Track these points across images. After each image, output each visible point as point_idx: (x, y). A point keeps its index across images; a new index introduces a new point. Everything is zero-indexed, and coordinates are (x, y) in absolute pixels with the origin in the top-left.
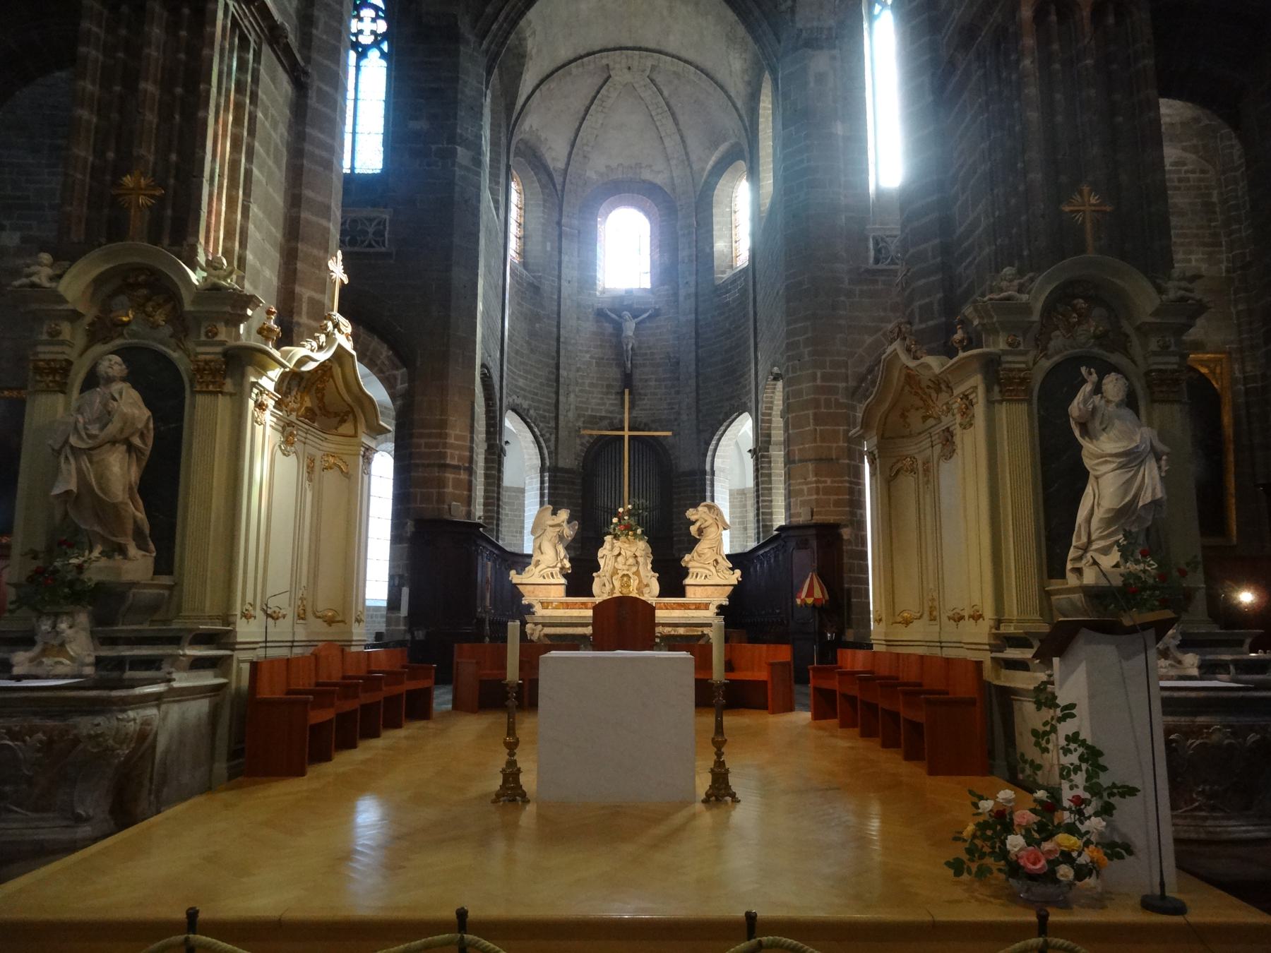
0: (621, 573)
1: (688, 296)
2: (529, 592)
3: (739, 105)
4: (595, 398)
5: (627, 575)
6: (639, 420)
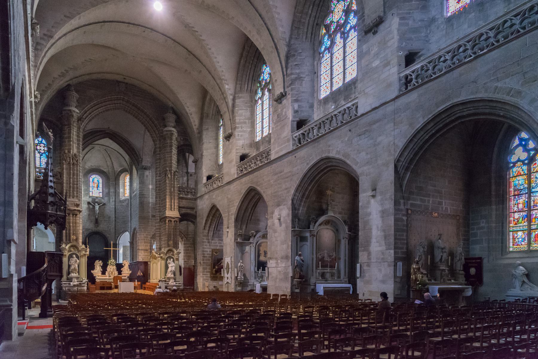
3: (128, 163)
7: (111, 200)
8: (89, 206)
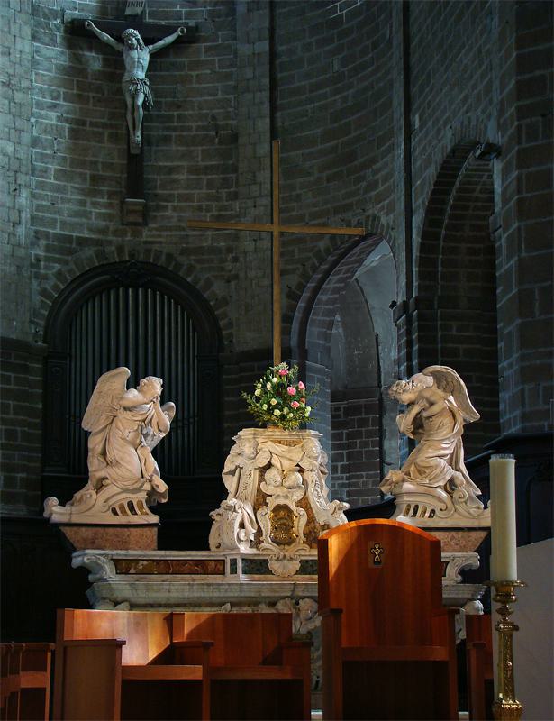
0: (272, 502)
2: (85, 540)
4: (69, 201)
5: (286, 507)
6: (156, 247)
8: (76, 58)
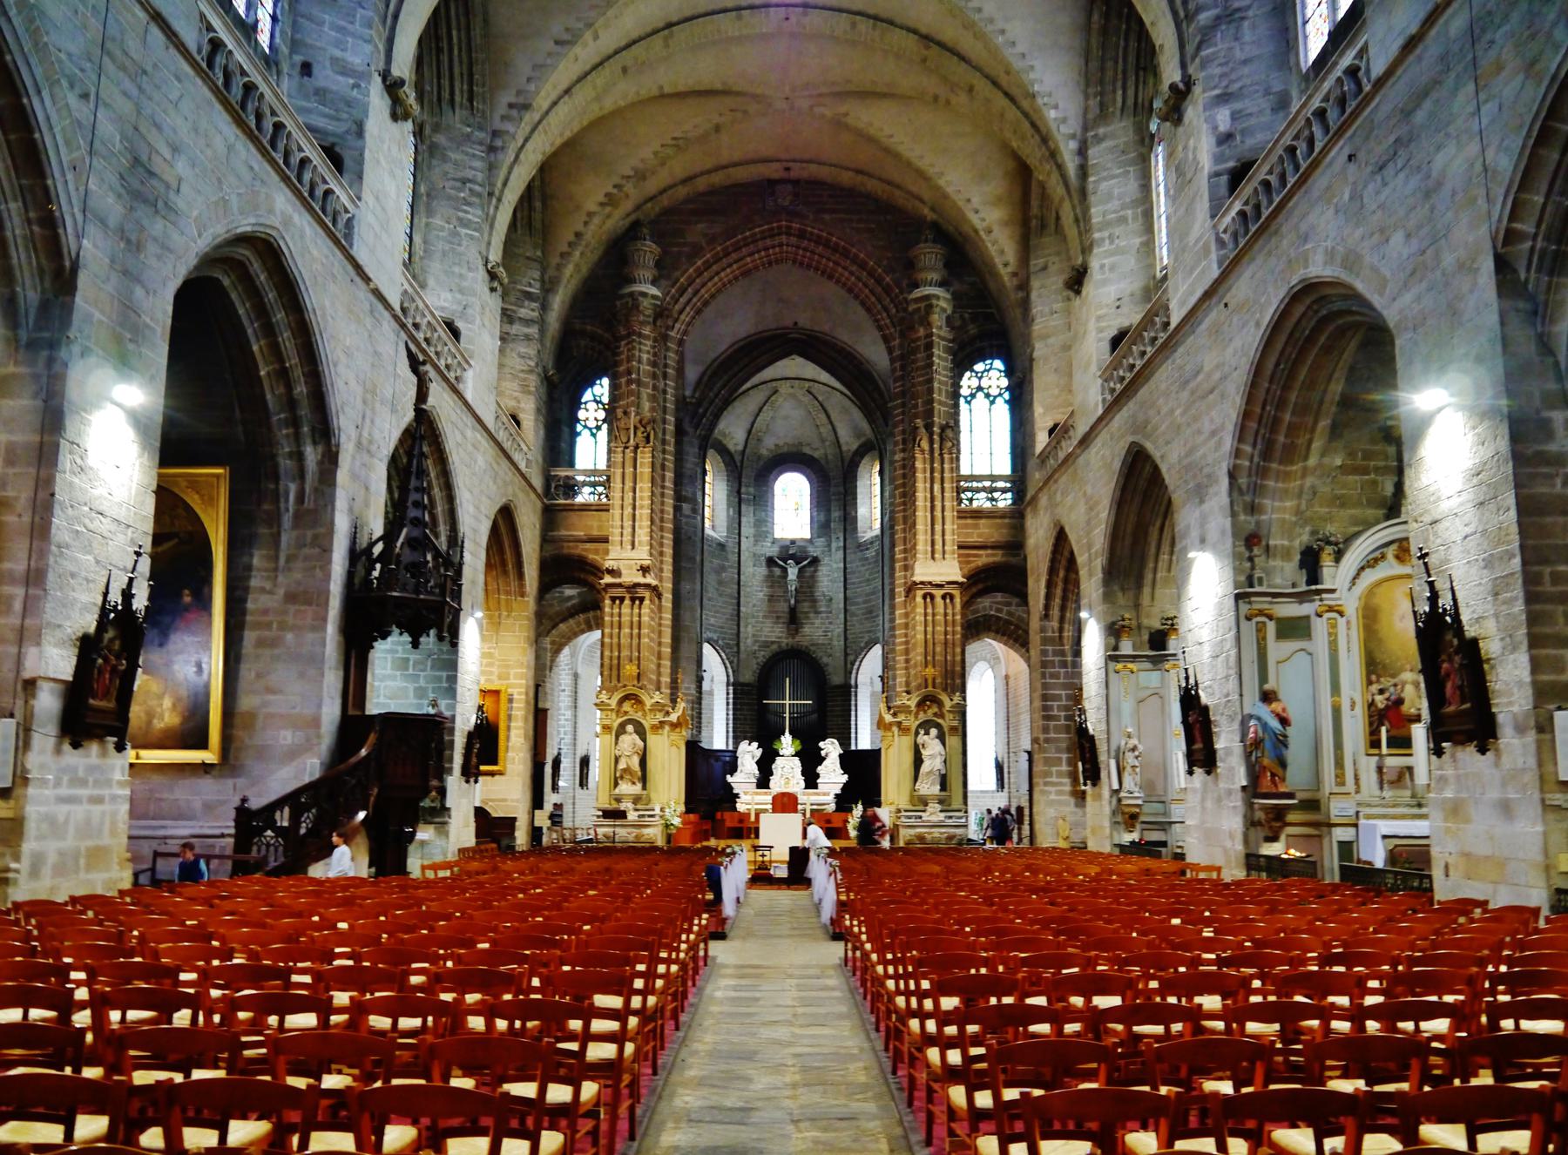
1: (838, 549)
7: (834, 545)
